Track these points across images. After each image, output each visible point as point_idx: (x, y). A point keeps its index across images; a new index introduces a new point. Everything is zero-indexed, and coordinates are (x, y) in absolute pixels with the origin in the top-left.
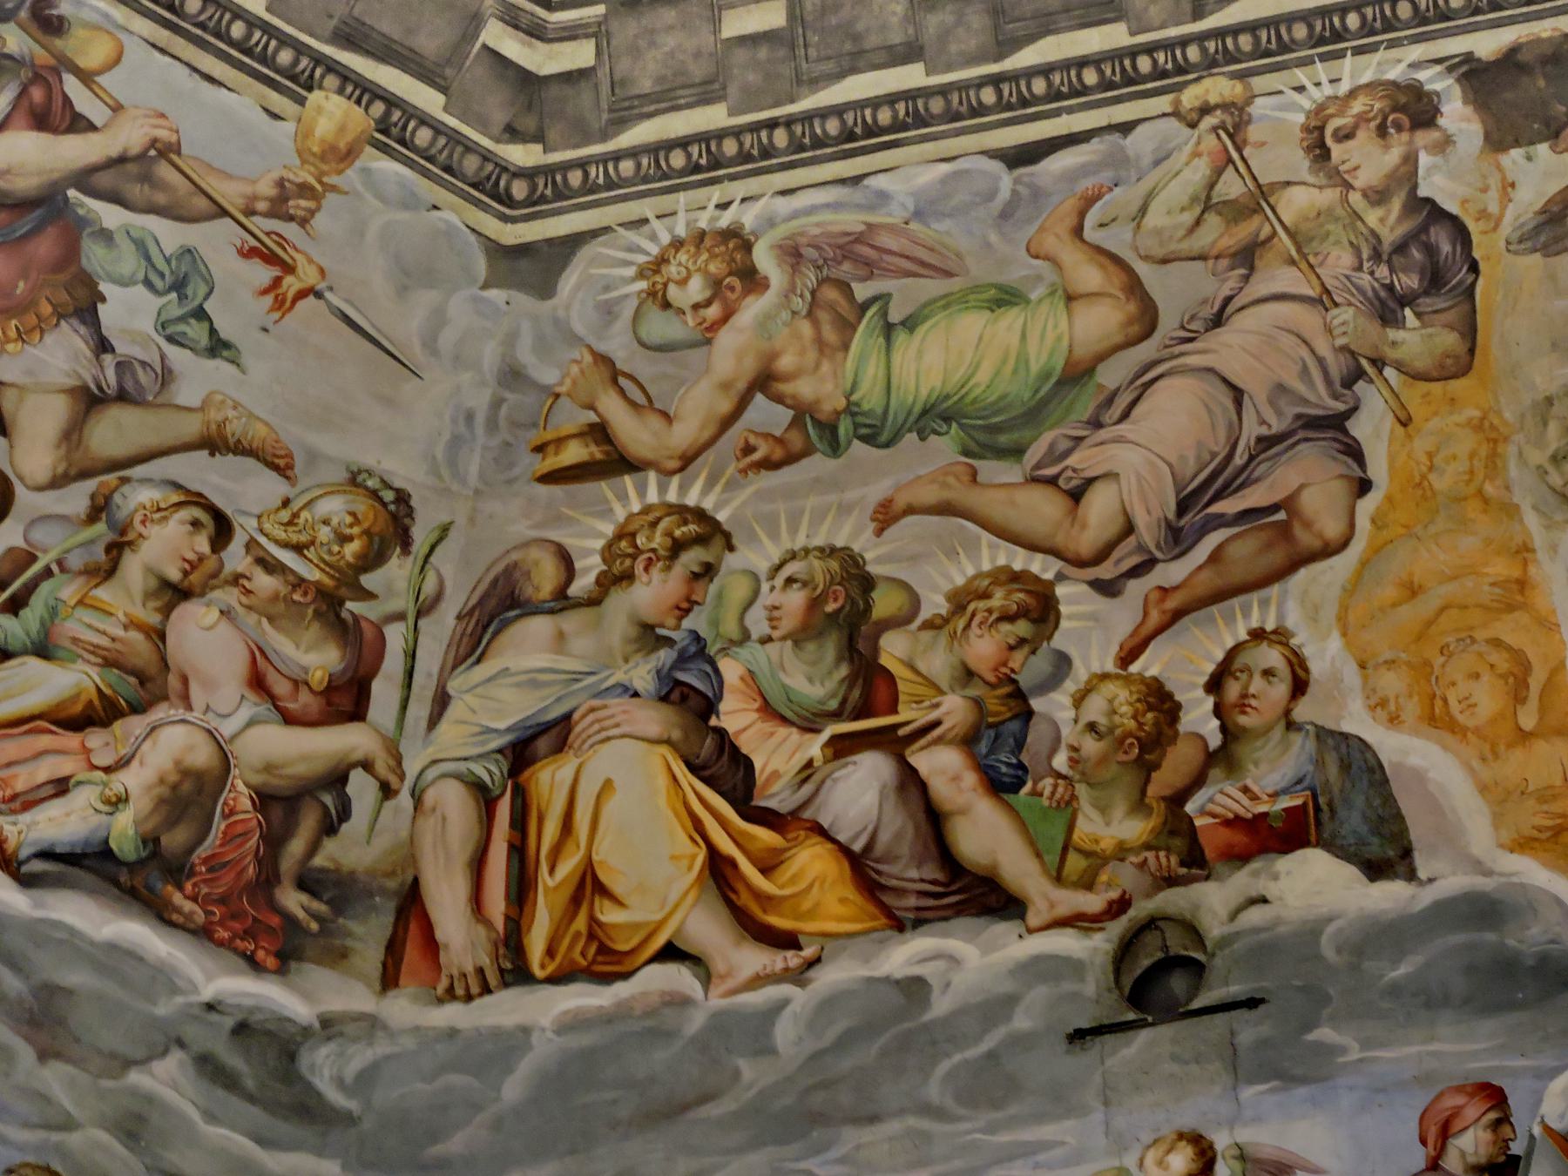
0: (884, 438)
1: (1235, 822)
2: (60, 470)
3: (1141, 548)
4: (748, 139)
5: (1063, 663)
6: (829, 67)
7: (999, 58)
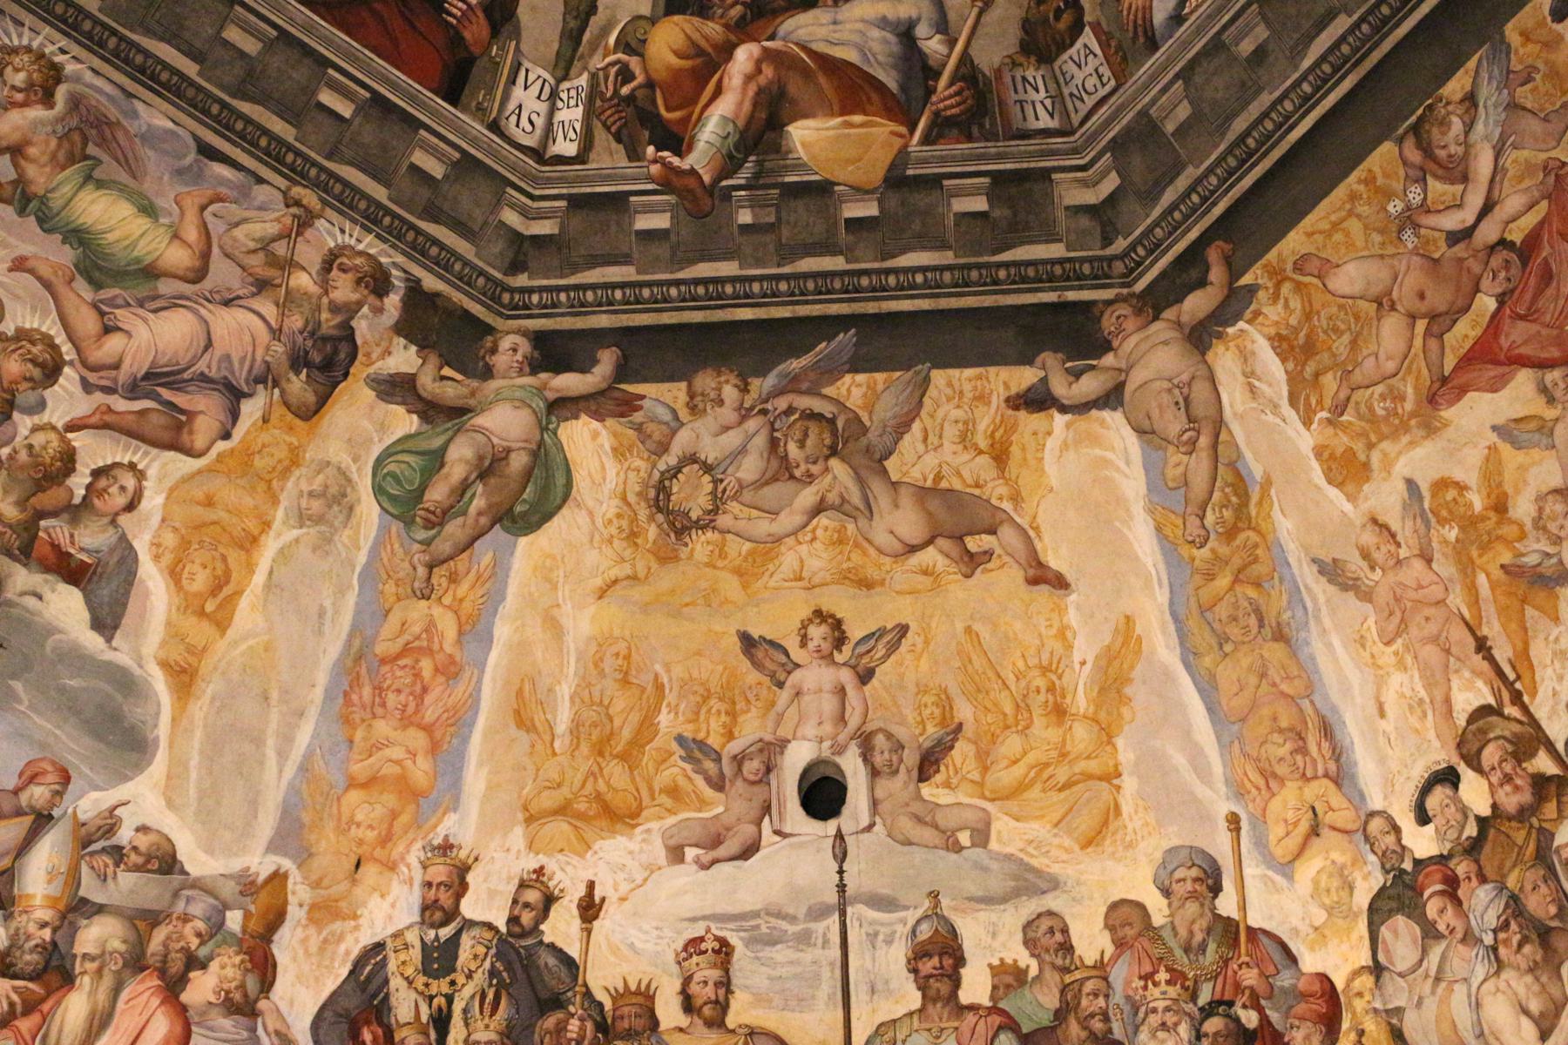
0: (46, 226)
1: (56, 547)
3: (115, 380)
5: (42, 405)
7: (234, 96)
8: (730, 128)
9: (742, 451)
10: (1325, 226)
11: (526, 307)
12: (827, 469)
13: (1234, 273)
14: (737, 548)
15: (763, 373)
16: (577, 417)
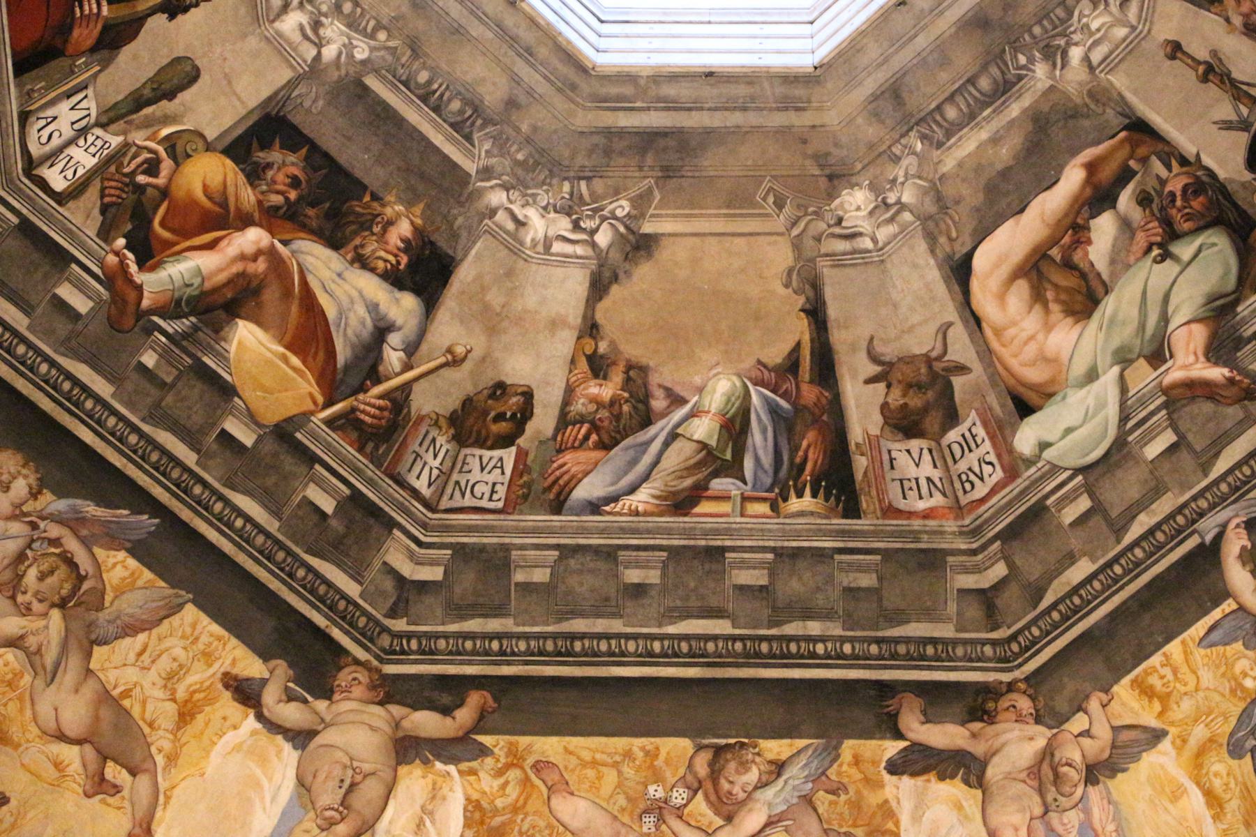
8: (197, 282)
10: (587, 756)
12: (45, 615)
13: (481, 724)
15: (60, 494)
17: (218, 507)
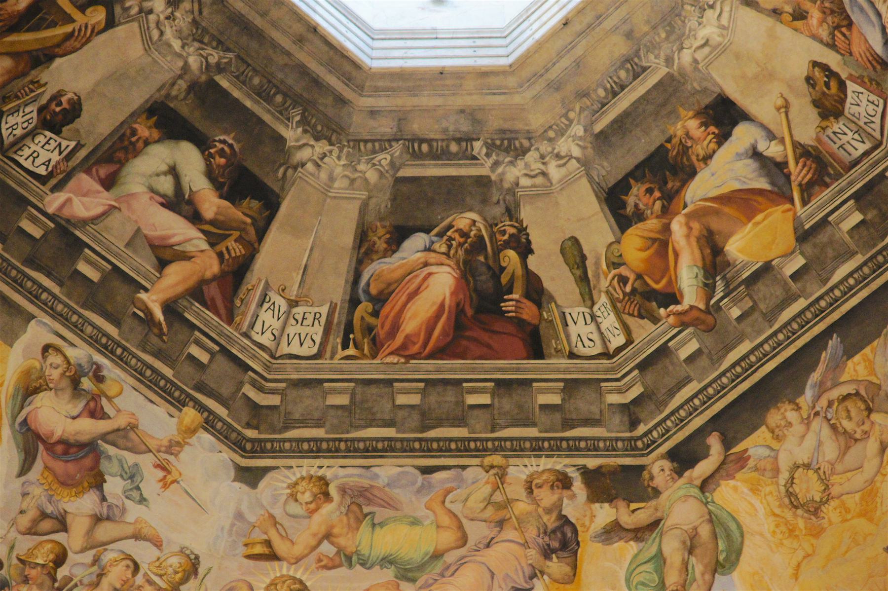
0: (368, 566)
2: (84, 546)
4: (331, 443)
6: (362, 423)
7: (422, 432)
8: (696, 270)
9: (820, 444)
11: (654, 442)
14: (852, 501)
15: (801, 392)
16: (719, 485)
17: (837, 293)
